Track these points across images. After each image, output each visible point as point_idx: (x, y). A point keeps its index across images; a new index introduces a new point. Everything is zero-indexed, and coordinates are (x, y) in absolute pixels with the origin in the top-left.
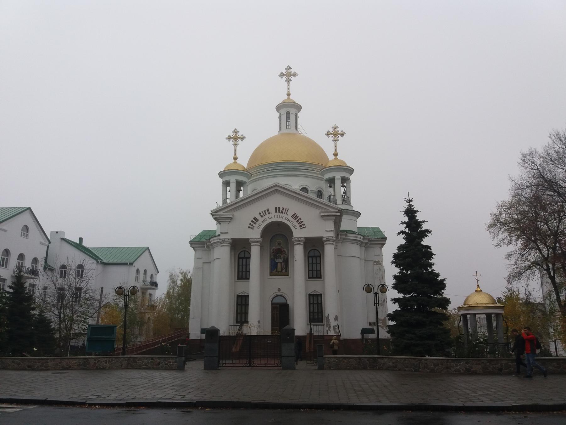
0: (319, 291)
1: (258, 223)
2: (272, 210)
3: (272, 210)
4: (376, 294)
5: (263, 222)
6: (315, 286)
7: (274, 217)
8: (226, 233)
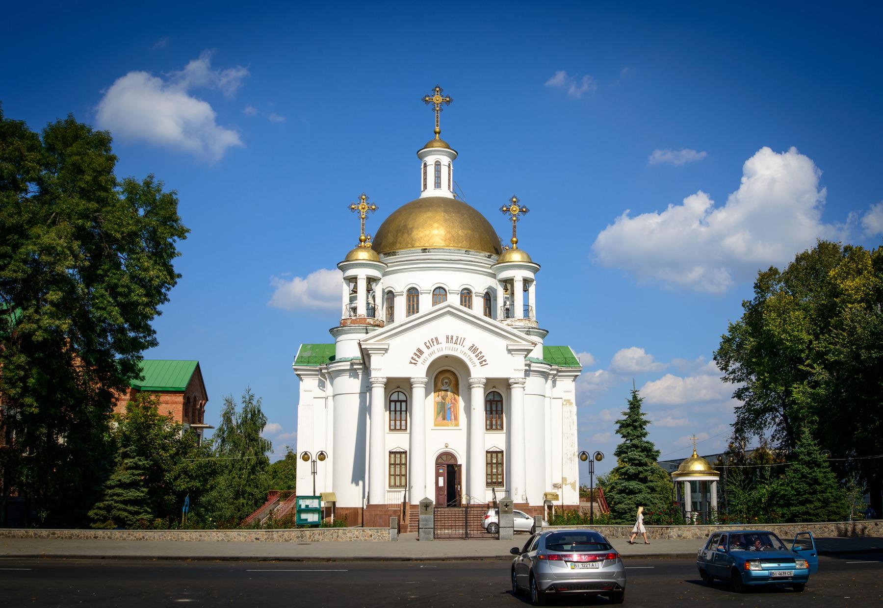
1: (423, 357)
3: (442, 339)
4: (591, 462)
7: (444, 349)
8: (380, 369)
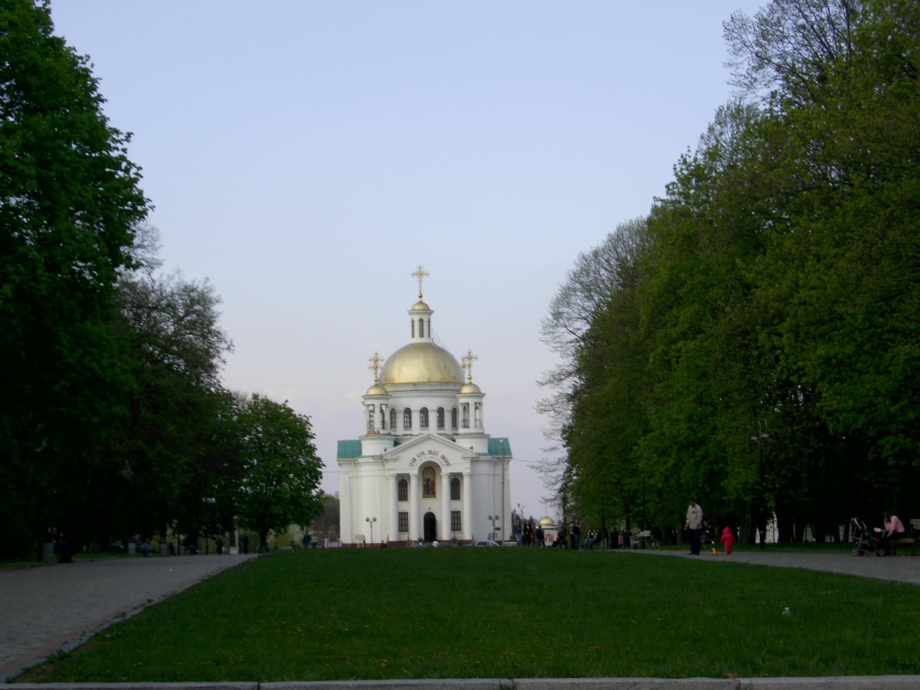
0: (458, 509)
2: (427, 453)
3: (427, 453)
6: (456, 505)
7: (428, 458)
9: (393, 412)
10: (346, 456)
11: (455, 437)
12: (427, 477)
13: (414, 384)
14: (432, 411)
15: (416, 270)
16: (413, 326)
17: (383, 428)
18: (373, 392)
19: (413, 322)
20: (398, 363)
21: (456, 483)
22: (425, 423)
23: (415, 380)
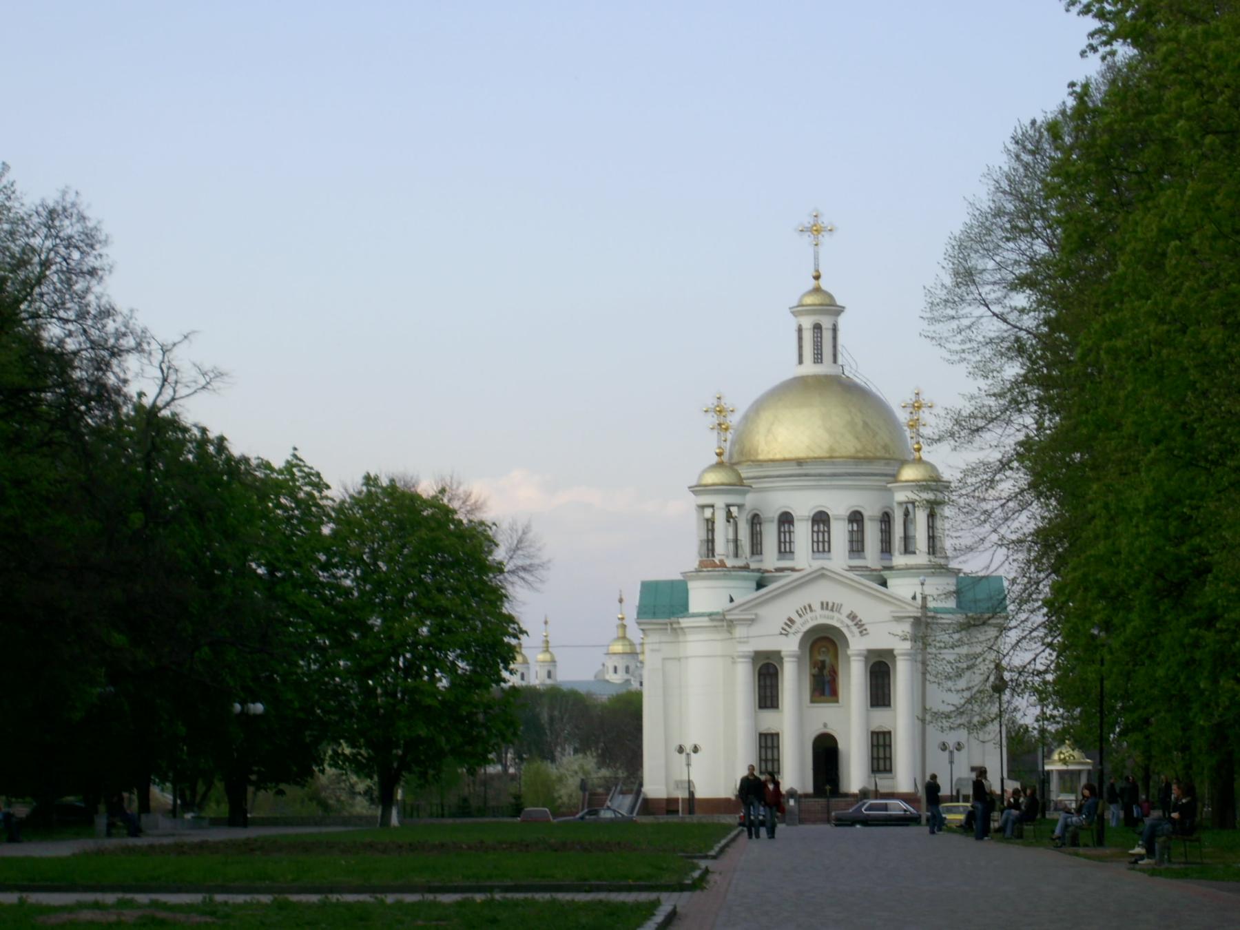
1: (795, 628)
2: (816, 606)
3: (816, 606)
5: (804, 623)
6: (881, 718)
7: (819, 618)
9: (756, 521)
10: (654, 615)
11: (886, 573)
12: (821, 658)
13: (800, 462)
14: (838, 518)
15: (807, 221)
16: (800, 339)
17: (736, 555)
18: (711, 478)
19: (800, 330)
20: (766, 417)
21: (880, 672)
22: (822, 545)
23: (801, 453)
